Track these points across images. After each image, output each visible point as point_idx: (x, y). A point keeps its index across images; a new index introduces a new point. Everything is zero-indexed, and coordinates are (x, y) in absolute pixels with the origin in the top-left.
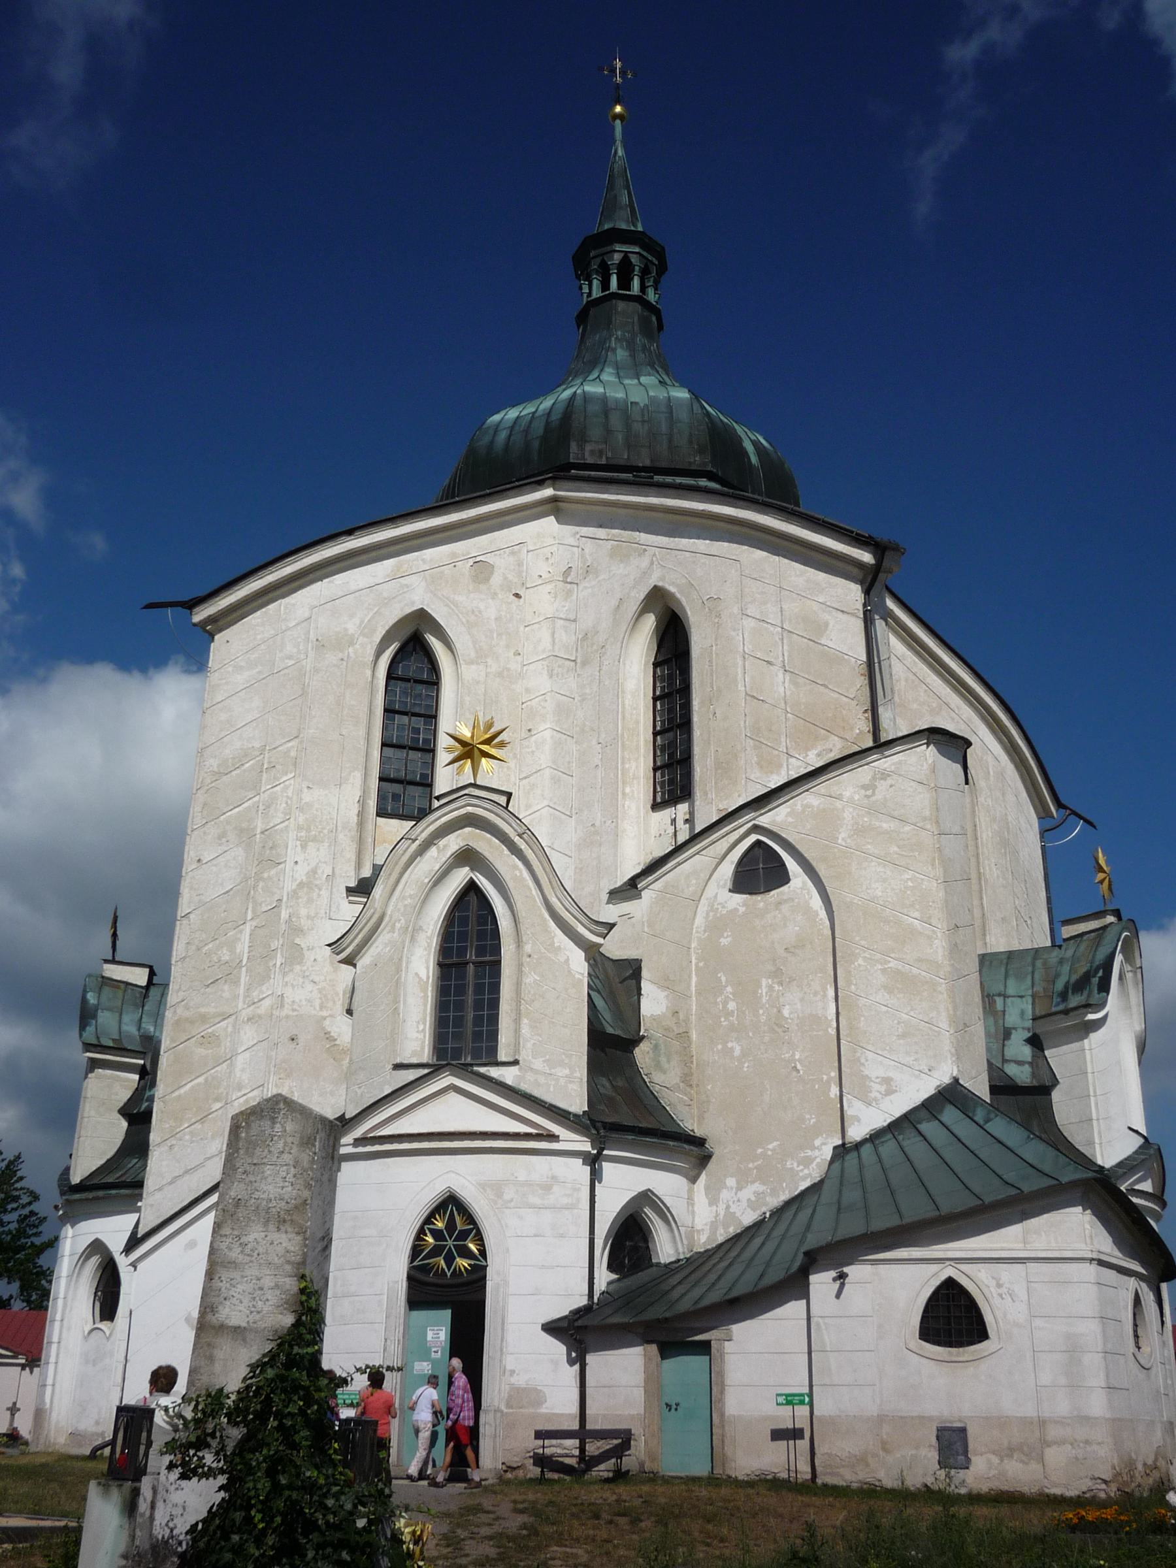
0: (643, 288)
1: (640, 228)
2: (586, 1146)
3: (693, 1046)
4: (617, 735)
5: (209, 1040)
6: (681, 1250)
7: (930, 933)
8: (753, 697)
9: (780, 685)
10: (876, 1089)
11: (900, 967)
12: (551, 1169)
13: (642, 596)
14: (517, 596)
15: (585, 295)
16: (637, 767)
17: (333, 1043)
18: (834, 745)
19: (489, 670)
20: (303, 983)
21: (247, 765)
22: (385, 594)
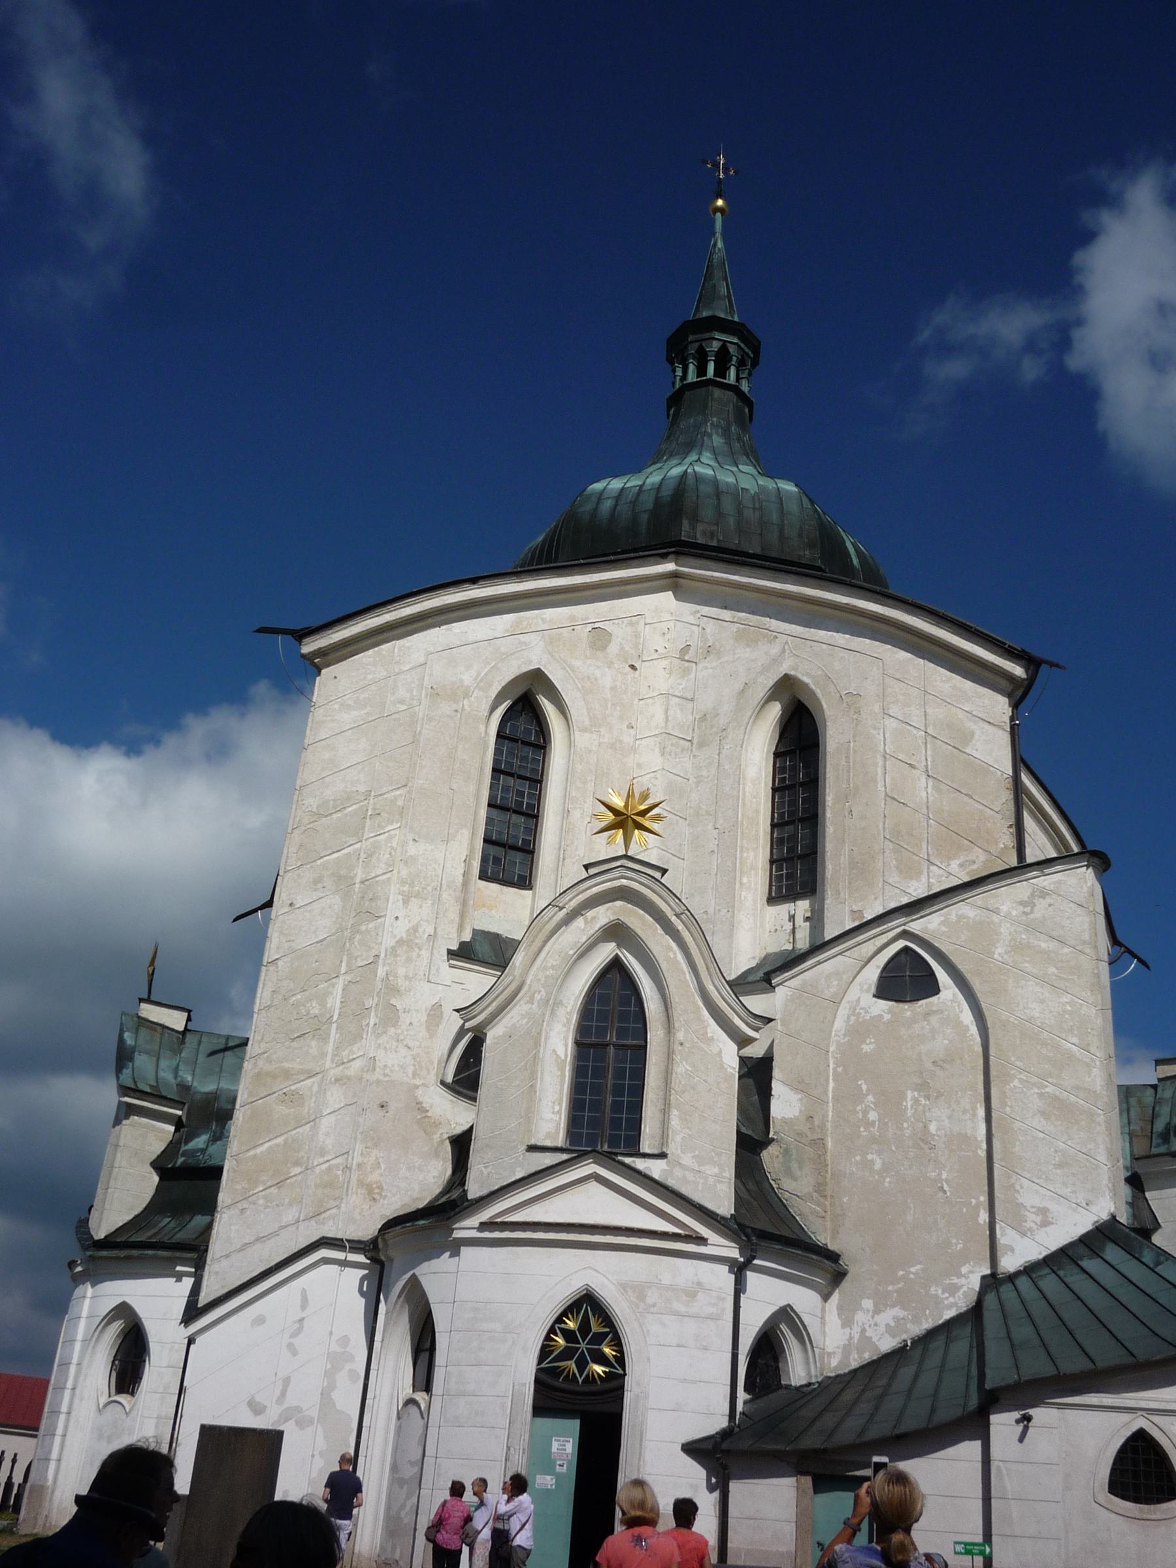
0: (738, 379)
1: (736, 319)
2: (733, 1251)
3: (829, 1154)
4: (737, 822)
5: (293, 1098)
6: (813, 1372)
7: (1088, 1060)
8: (894, 799)
9: (922, 790)
10: (1032, 1219)
11: (1058, 1093)
12: (697, 1275)
13: (771, 683)
14: (633, 667)
15: (678, 378)
16: (755, 857)
17: (424, 1115)
18: (977, 857)
19: (601, 740)
20: (397, 1047)
21: (350, 809)
22: (503, 649)
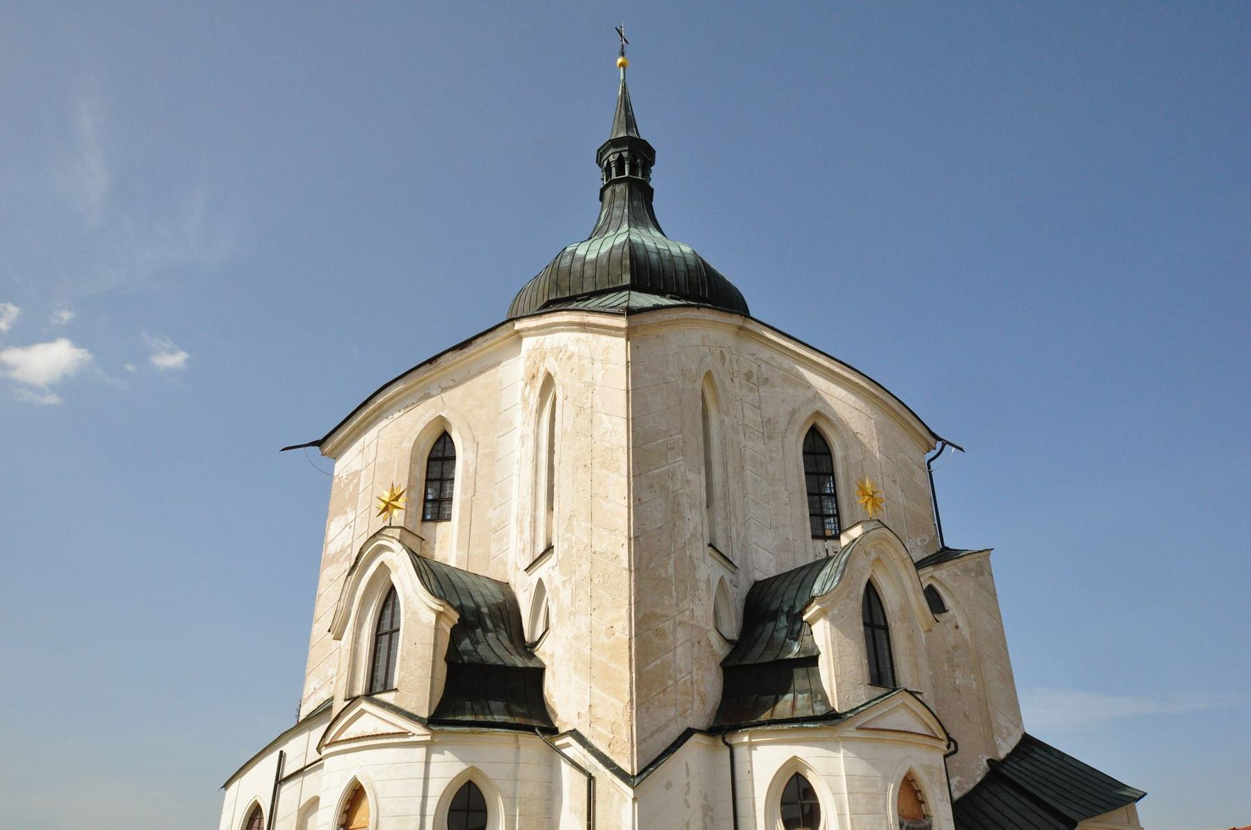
13: (809, 413)
21: (660, 441)
